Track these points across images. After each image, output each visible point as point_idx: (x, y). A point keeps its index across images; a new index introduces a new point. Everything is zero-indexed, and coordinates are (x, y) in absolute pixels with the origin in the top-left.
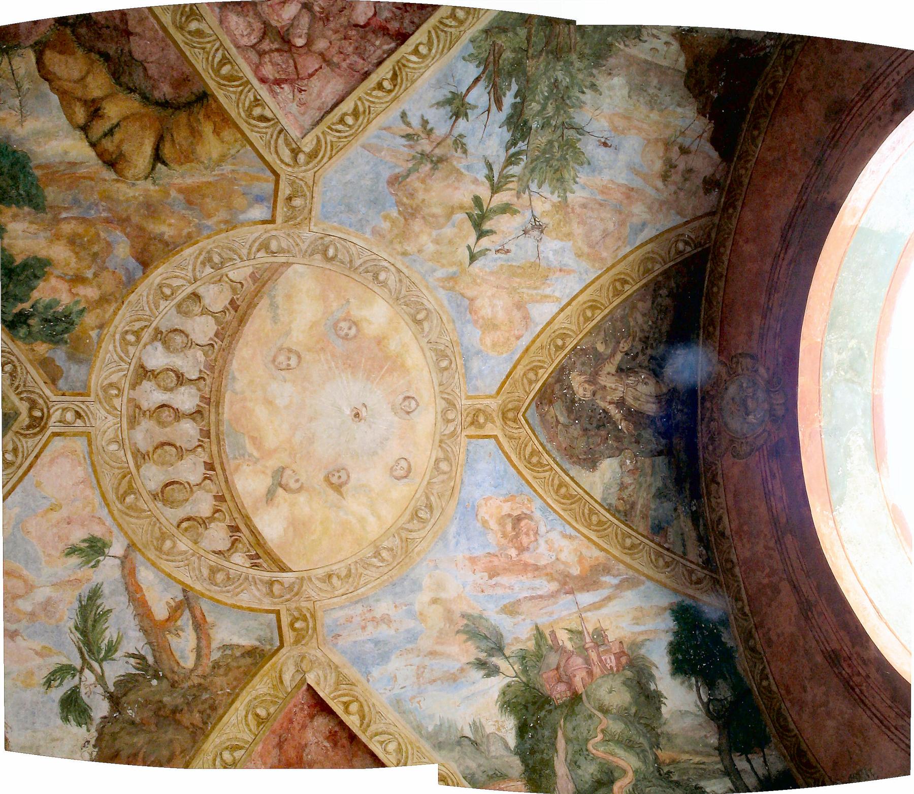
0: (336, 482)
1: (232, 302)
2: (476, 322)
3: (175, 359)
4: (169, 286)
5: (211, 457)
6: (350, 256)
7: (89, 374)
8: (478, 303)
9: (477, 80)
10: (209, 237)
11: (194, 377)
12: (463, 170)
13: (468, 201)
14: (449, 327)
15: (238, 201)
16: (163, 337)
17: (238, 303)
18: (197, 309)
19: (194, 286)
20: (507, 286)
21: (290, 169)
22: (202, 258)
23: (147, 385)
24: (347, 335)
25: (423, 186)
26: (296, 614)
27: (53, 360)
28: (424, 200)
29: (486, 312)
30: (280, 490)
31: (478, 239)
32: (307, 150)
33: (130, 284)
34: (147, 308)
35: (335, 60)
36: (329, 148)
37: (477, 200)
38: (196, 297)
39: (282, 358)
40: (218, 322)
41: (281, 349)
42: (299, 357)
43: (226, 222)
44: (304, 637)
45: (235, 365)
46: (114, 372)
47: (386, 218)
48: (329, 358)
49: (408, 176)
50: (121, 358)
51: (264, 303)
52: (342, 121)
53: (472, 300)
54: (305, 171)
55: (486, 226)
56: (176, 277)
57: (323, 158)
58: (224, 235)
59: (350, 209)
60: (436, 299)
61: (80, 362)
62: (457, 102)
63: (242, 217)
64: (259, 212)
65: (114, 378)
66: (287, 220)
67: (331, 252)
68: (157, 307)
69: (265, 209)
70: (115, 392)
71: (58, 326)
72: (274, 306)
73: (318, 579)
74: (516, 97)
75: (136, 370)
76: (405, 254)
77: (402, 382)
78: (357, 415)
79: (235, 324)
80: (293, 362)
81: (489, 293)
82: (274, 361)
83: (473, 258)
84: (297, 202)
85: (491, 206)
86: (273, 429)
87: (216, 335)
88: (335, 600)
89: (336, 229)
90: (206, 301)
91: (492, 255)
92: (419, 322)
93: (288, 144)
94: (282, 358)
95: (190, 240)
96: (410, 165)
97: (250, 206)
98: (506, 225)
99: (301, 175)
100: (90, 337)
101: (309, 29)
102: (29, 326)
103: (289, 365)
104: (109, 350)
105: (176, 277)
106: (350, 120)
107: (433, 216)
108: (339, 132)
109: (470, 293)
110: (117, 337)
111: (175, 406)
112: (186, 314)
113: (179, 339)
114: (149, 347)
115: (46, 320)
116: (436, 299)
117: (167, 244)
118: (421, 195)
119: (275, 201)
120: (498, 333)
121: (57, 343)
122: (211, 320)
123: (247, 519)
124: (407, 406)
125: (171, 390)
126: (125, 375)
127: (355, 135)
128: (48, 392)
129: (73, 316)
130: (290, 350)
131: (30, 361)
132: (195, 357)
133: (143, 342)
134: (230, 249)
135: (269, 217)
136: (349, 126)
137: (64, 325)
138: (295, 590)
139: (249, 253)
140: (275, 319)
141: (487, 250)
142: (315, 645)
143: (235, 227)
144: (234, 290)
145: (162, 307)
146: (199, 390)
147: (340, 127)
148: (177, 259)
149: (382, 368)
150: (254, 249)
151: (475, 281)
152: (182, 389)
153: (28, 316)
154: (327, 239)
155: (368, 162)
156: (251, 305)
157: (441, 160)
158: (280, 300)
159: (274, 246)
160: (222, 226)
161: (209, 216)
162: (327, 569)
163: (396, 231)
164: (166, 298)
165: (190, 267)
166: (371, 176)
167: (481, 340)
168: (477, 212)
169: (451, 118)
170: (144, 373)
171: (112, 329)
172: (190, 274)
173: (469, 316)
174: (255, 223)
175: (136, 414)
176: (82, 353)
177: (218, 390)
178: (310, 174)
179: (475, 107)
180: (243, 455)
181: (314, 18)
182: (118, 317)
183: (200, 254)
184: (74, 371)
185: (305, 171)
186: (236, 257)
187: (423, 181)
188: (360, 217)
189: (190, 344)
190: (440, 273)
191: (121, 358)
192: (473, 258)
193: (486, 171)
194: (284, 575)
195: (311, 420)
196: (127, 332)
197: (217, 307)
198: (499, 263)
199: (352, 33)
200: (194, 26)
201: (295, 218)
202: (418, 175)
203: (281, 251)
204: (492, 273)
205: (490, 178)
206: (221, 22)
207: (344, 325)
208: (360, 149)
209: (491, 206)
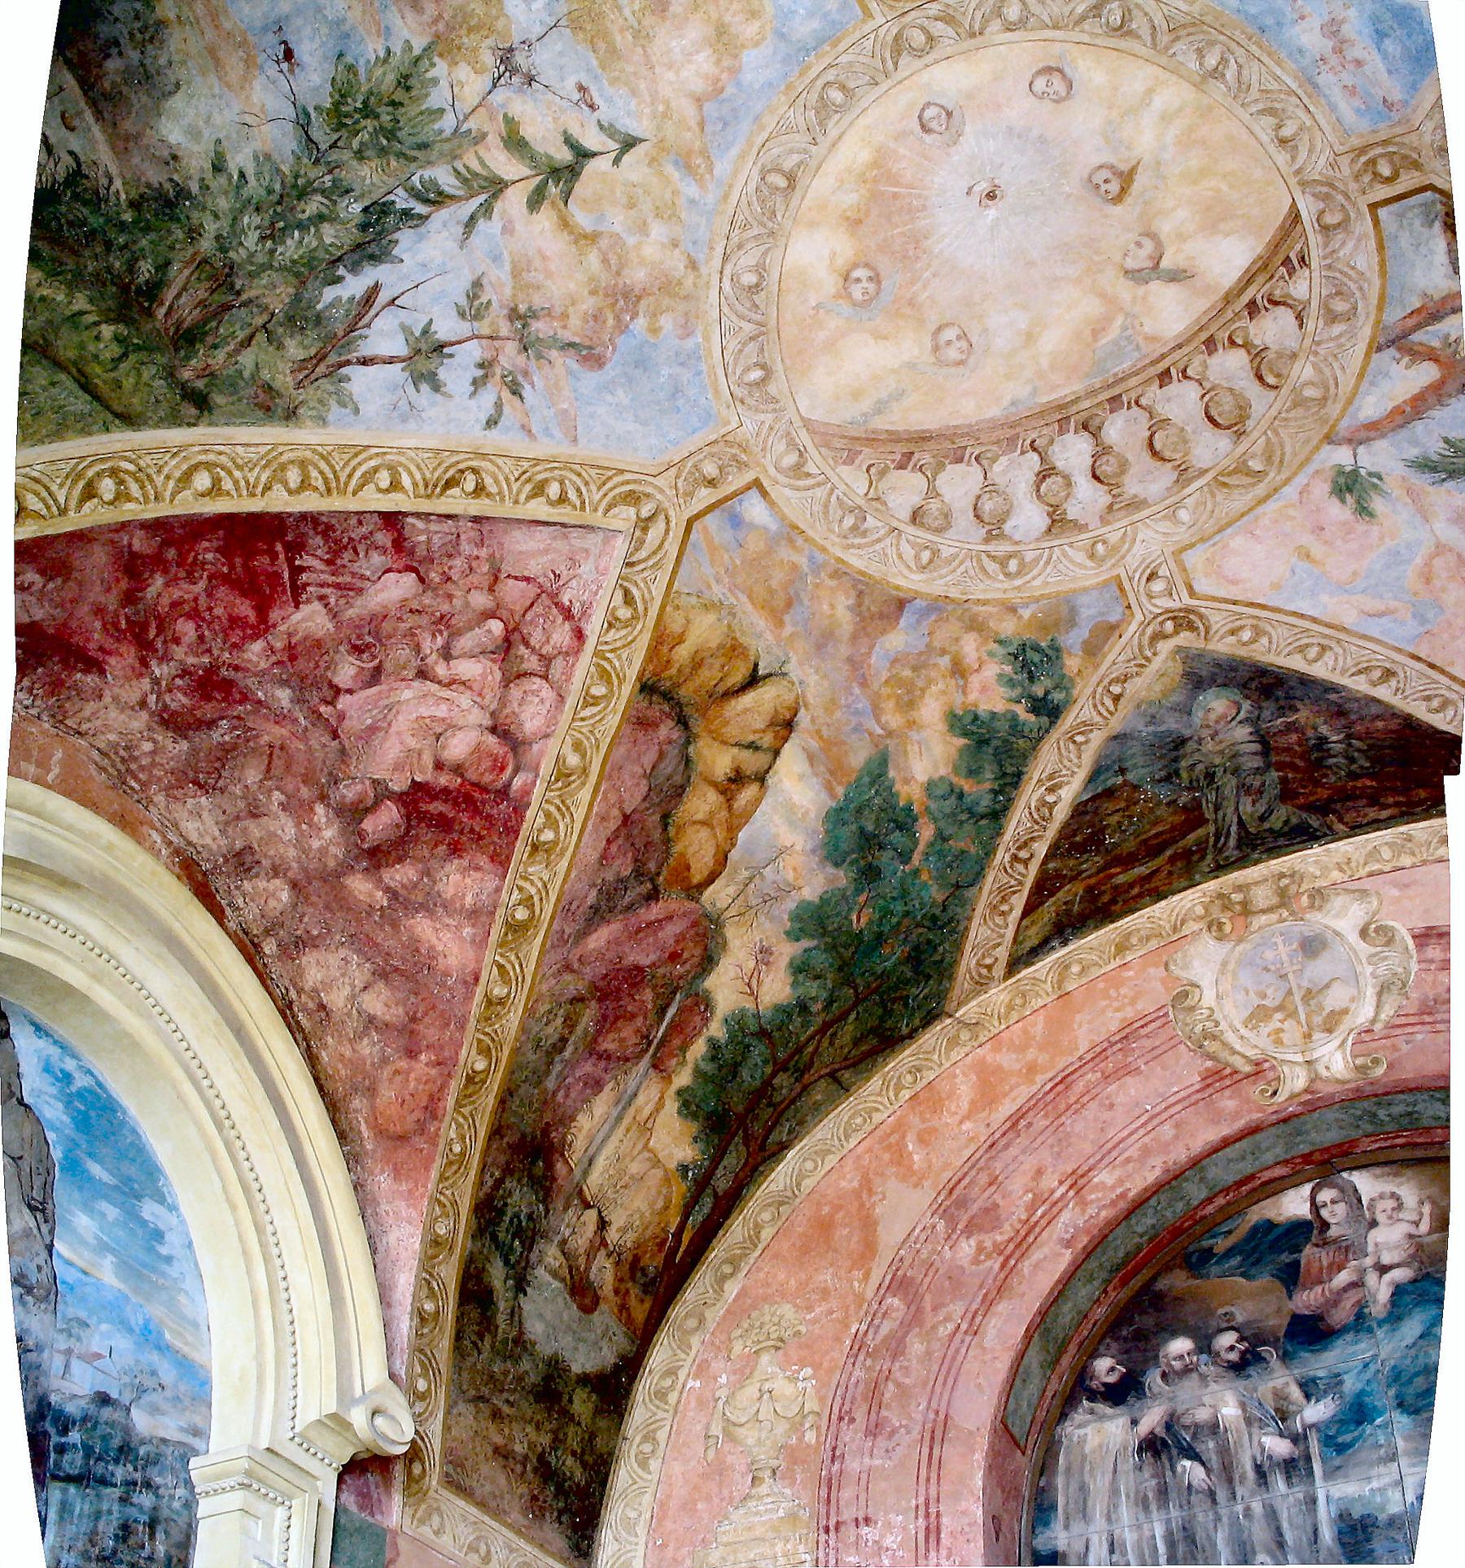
0: (1119, 183)
1: (901, 466)
2: (734, 71)
3: (1020, 495)
4: (917, 557)
5: (1148, 381)
6: (744, 344)
7: (1085, 590)
8: (699, 86)
9: (365, 362)
10: (824, 550)
11: (1036, 457)
12: (508, 267)
13: (545, 218)
14: (770, 123)
15: (755, 544)
16: (994, 527)
17: (898, 457)
18: (934, 505)
19: (902, 526)
20: (639, 50)
21: (672, 513)
22: (857, 541)
23: (1072, 511)
24: (870, 279)
25: (571, 310)
26: (1367, 178)
27: (1085, 642)
28: (593, 293)
29: (704, 61)
30: (1164, 264)
31: (594, 155)
32: (632, 511)
33: (938, 606)
34: (962, 569)
35: (485, 568)
36: (609, 485)
37: (535, 201)
38: (916, 517)
39: (952, 354)
40: (941, 466)
41: (941, 363)
42: (939, 329)
43: (791, 541)
44: (1404, 157)
45: (994, 412)
46: (1072, 561)
47: (654, 331)
48: (919, 285)
49: (571, 345)
50: (1047, 563)
51: (881, 423)
52: (563, 499)
53: (699, 101)
54: (661, 491)
55: (565, 156)
56: (900, 557)
57: (628, 482)
58: (810, 533)
59: (677, 391)
60: (735, 173)
61: (1073, 611)
62: (422, 365)
63: (773, 526)
64: (754, 509)
65: (1080, 557)
66: (742, 466)
67: (756, 374)
68: (954, 557)
69: (745, 504)
70: (1100, 547)
71: (1032, 658)
72: (880, 408)
73: (1293, 158)
74: (339, 280)
75: (1057, 536)
76: (693, 265)
77: (902, 151)
78: (991, 196)
79: (932, 445)
80: (950, 334)
81: (671, 76)
82: (961, 363)
83: (629, 143)
84: (710, 470)
85: (527, 172)
86: (1067, 313)
87: (960, 460)
88: (1322, 122)
89: (717, 391)
90: (917, 500)
91: (605, 113)
92: (791, 179)
93: (642, 542)
94: (952, 354)
95: (841, 572)
96: (554, 354)
97: (752, 526)
98: (543, 126)
99: (672, 493)
100: (1034, 616)
101: (472, 629)
102: (1047, 693)
103: (959, 338)
104: (1045, 582)
105: (900, 557)
106: (554, 490)
107: (605, 261)
108: (578, 490)
109: (690, 111)
110: (1018, 582)
111: (1090, 461)
112: (947, 515)
113: (987, 506)
114: (1017, 537)
115: (1032, 678)
116: (735, 170)
117: (860, 594)
118: (588, 304)
119: (727, 498)
120: (727, 19)
121: (1058, 650)
122: (942, 480)
123: (1228, 299)
124: (939, 122)
125: (1067, 478)
126: (1071, 545)
127: (567, 465)
128: (1133, 627)
129: (1012, 649)
130: (936, 348)
131: (1097, 666)
132: (1004, 472)
133: (1011, 548)
134: (826, 512)
135: (754, 494)
136: (562, 483)
137: (1030, 654)
138: (1325, 189)
139: (819, 485)
140: (900, 395)
141: (601, 127)
142: (1414, 137)
143: (795, 527)
144: (883, 473)
145: (952, 551)
146: (1052, 442)
147: (572, 495)
148: (874, 569)
149: (895, 196)
150: (810, 482)
151: (665, 115)
152: (1060, 464)
153: (1033, 699)
154: (739, 392)
155: (592, 416)
156: (894, 437)
157: (514, 315)
158: (866, 405)
159: (791, 459)
160: (800, 542)
161: (795, 567)
162: (1272, 149)
163: (666, 302)
164: (936, 553)
165: (877, 547)
166: (609, 398)
167: (757, 44)
168: (553, 190)
169: (451, 356)
170: (1058, 522)
171: (1009, 595)
172: (888, 541)
173: (730, 90)
174: (772, 504)
175: (1121, 505)
176: (1063, 613)
177: (1041, 414)
178: (659, 481)
179: (406, 329)
180: (1128, 338)
181: (456, 634)
182: (989, 596)
183: (853, 546)
184: (1089, 612)
185: (661, 491)
186: (833, 498)
187: (565, 316)
188: (678, 370)
189: (990, 488)
190: (691, 190)
191: (1047, 563)
192: (629, 143)
193: (481, 224)
194: (1304, 214)
195: (1031, 264)
196: (1007, 575)
197: (918, 481)
198: (611, 90)
199: (434, 576)
200: (573, 760)
201: (735, 458)
202: (560, 332)
203: (792, 444)
204: (634, 93)
205: (487, 210)
206: (547, 736)
207: (857, 292)
208: (582, 441)
209: (527, 172)
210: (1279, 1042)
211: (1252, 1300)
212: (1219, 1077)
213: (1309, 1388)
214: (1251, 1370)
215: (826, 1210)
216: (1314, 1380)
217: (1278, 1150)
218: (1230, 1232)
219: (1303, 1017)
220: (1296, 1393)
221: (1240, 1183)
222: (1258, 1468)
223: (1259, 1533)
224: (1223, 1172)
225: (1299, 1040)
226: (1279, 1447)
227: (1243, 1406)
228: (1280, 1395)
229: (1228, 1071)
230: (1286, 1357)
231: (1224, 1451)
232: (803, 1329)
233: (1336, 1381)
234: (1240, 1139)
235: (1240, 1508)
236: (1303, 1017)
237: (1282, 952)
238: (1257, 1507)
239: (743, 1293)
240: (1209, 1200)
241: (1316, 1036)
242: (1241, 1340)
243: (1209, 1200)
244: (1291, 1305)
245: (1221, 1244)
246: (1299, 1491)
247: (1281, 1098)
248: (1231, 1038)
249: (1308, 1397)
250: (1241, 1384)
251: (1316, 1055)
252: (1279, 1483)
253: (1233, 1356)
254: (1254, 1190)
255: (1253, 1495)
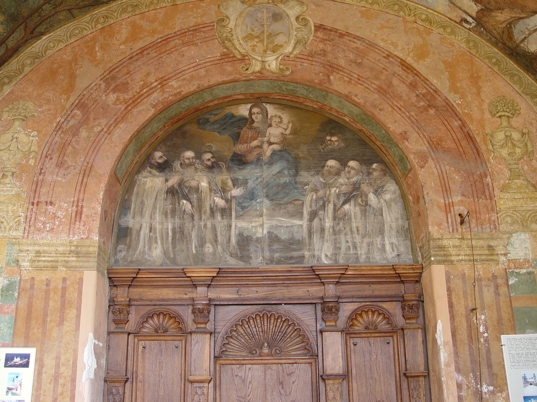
210: (253, 50)
211: (220, 143)
212: (227, 57)
213: (236, 183)
214: (215, 170)
215: (56, 66)
216: (237, 180)
217: (242, 90)
218: (216, 115)
219: (265, 43)
220: (230, 183)
221: (226, 97)
222: (211, 209)
223: (209, 235)
224: (220, 92)
225: (262, 52)
226: (221, 202)
227: (209, 183)
228: (224, 183)
229: (232, 55)
230: (229, 169)
231: (200, 200)
232: (36, 114)
233: (245, 182)
234: (230, 83)
235: (202, 224)
236: (265, 43)
237: (265, 15)
238: (209, 225)
239: (12, 92)
240: (212, 101)
241: (268, 52)
242: (213, 157)
243: (212, 101)
244: (234, 149)
245: (212, 118)
246: (225, 222)
247: (249, 72)
248: (236, 42)
249: (234, 185)
250: (210, 174)
251: (266, 59)
252: (219, 218)
253: (209, 163)
254: (230, 101)
255: (208, 219)
